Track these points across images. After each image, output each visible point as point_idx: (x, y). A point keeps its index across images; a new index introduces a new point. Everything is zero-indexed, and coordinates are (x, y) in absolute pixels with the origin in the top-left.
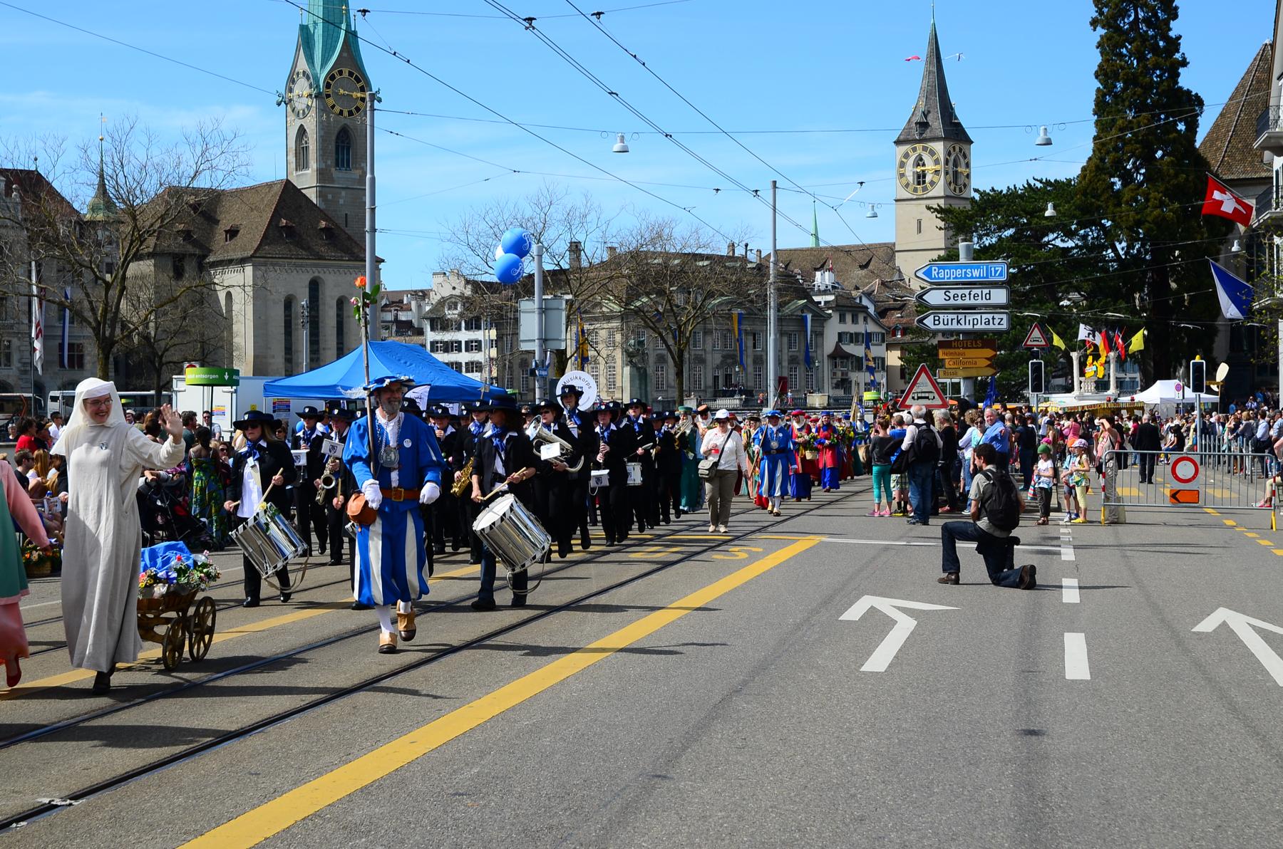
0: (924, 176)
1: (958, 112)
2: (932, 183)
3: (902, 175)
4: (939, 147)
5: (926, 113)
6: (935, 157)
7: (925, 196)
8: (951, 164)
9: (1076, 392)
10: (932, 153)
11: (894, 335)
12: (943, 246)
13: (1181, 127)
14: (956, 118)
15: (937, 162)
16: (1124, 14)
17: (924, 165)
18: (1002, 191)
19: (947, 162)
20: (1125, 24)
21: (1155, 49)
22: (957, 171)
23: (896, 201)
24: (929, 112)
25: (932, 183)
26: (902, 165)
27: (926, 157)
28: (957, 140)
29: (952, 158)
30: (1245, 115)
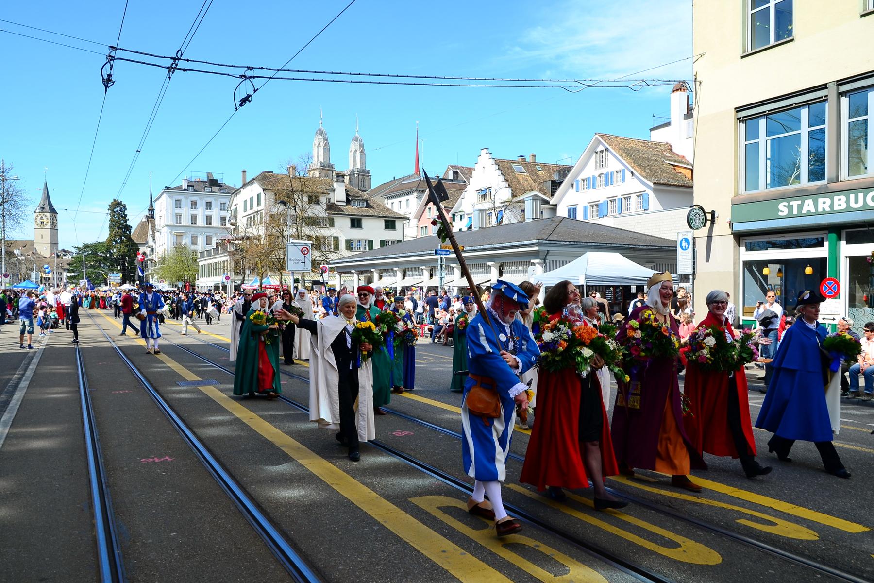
2: (46, 225)
3: (36, 222)
4: (48, 215)
10: (46, 216)
13: (128, 232)
15: (47, 219)
16: (115, 208)
19: (50, 219)
20: (115, 210)
21: (122, 216)
26: (36, 219)
27: (44, 217)
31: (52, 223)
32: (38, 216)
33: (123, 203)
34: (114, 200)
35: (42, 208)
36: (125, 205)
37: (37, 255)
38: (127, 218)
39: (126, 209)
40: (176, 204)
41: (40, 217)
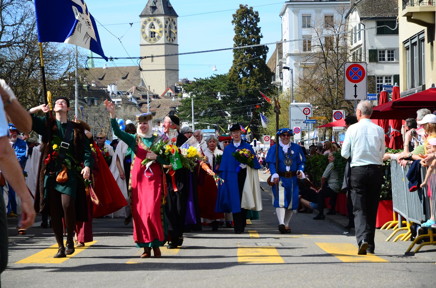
0: (155, 33)
4: (162, 19)
5: (155, 1)
6: (160, 24)
7: (155, 43)
10: (158, 22)
12: (164, 68)
13: (261, 57)
14: (170, 5)
15: (161, 26)
16: (243, 19)
20: (243, 22)
21: (253, 32)
23: (141, 45)
25: (159, 37)
27: (155, 24)
29: (168, 24)
31: (168, 34)
33: (254, 10)
34: (241, 7)
36: (257, 13)
38: (260, 34)
39: (258, 20)
40: (304, 21)
41: (149, 24)
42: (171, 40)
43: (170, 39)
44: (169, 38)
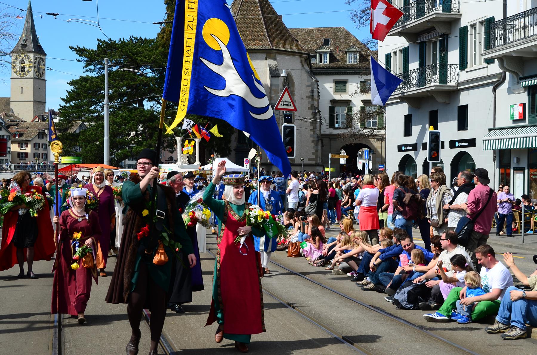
0: (24, 68)
1: (40, 41)
2: (28, 72)
4: (32, 56)
5: (26, 40)
7: (24, 77)
8: (37, 63)
9: (179, 163)
10: (28, 58)
11: (15, 137)
14: (39, 44)
17: (24, 63)
18: (115, 41)
19: (35, 63)
22: (39, 67)
23: (11, 78)
24: (27, 40)
25: (28, 72)
28: (40, 53)
29: (37, 61)
30: (241, 15)
31: (36, 69)
32: (16, 59)
35: (23, 45)
37: (12, 118)
41: (20, 59)
42: (39, 75)
43: (38, 74)
44: (37, 74)
